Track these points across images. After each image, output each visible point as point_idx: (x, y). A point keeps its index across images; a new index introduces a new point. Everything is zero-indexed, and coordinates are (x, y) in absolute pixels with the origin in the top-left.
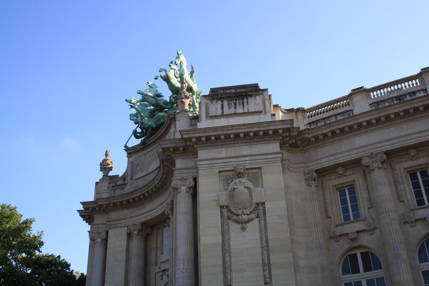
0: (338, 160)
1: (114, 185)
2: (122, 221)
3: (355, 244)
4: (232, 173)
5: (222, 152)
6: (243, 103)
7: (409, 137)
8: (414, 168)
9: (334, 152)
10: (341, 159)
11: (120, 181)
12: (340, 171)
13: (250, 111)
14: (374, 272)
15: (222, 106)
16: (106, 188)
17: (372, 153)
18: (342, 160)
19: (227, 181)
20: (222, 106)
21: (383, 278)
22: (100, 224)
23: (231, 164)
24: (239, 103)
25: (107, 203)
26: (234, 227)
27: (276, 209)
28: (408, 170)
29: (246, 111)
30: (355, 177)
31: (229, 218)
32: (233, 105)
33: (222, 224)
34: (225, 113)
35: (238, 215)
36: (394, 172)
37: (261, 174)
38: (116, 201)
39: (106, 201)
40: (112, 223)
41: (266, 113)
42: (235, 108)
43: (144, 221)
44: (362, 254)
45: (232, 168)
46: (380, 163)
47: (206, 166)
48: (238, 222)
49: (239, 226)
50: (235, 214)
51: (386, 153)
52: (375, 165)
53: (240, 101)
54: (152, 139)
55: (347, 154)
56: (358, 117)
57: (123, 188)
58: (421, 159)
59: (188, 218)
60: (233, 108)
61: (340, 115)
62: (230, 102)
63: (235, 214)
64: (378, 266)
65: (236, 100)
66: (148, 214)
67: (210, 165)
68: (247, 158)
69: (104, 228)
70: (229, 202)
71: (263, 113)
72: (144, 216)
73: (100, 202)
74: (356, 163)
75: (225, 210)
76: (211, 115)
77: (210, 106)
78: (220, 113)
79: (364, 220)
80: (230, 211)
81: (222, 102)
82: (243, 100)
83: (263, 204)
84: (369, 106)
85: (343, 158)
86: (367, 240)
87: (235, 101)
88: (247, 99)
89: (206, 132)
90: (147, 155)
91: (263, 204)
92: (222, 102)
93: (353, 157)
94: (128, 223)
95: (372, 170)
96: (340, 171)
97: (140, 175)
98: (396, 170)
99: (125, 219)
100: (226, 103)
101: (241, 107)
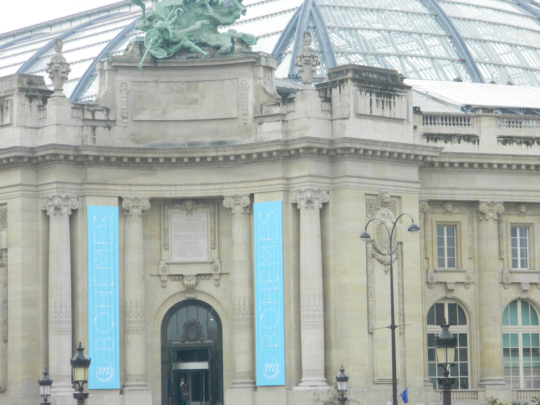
0: (452, 196)
1: (91, 118)
2: (110, 187)
3: (450, 295)
4: (374, 198)
6: (390, 102)
7: (528, 193)
8: (516, 225)
9: (452, 185)
10: (457, 196)
11: (100, 113)
12: (449, 207)
13: (396, 117)
14: (458, 326)
15: (371, 100)
16: (69, 117)
17: (493, 202)
18: (458, 198)
19: (371, 208)
20: (371, 100)
21: (466, 334)
22: (69, 183)
23: (376, 188)
24: (387, 101)
25: (96, 154)
28: (513, 225)
29: (393, 116)
31: (373, 257)
32: (381, 103)
33: (367, 260)
34: (373, 114)
35: (383, 254)
36: (501, 224)
37: (401, 205)
38: (111, 154)
39: (96, 151)
40: (93, 186)
41: (408, 122)
42: (383, 108)
43: (154, 196)
44: (449, 305)
45: (376, 193)
46: (496, 214)
47: (354, 184)
48: (382, 262)
49: (382, 267)
50: (379, 252)
51: (506, 204)
52: (491, 214)
53: (385, 99)
54: (176, 62)
55: (466, 192)
56: (493, 157)
57: (109, 128)
58: (527, 217)
60: (381, 108)
61: (464, 139)
62: (378, 99)
63: (379, 252)
64: (463, 322)
65: (384, 98)
66: (164, 188)
67: (357, 185)
68: (391, 183)
69: (73, 191)
70: (375, 237)
71: (405, 121)
72: (155, 188)
73: (86, 150)
75: (370, 246)
76: (360, 112)
77: (360, 98)
78: (368, 113)
79: (465, 272)
80: (374, 248)
81: (371, 95)
82: (390, 98)
83: (402, 243)
84: (496, 139)
86: (463, 295)
87: (382, 98)
88: (394, 99)
89: (367, 144)
90: (162, 86)
91: (402, 243)
92: (371, 95)
94: (121, 192)
95: (487, 220)
96: (449, 207)
97: (145, 116)
98: (502, 222)
99: (116, 184)
100: (374, 97)
101: (388, 108)
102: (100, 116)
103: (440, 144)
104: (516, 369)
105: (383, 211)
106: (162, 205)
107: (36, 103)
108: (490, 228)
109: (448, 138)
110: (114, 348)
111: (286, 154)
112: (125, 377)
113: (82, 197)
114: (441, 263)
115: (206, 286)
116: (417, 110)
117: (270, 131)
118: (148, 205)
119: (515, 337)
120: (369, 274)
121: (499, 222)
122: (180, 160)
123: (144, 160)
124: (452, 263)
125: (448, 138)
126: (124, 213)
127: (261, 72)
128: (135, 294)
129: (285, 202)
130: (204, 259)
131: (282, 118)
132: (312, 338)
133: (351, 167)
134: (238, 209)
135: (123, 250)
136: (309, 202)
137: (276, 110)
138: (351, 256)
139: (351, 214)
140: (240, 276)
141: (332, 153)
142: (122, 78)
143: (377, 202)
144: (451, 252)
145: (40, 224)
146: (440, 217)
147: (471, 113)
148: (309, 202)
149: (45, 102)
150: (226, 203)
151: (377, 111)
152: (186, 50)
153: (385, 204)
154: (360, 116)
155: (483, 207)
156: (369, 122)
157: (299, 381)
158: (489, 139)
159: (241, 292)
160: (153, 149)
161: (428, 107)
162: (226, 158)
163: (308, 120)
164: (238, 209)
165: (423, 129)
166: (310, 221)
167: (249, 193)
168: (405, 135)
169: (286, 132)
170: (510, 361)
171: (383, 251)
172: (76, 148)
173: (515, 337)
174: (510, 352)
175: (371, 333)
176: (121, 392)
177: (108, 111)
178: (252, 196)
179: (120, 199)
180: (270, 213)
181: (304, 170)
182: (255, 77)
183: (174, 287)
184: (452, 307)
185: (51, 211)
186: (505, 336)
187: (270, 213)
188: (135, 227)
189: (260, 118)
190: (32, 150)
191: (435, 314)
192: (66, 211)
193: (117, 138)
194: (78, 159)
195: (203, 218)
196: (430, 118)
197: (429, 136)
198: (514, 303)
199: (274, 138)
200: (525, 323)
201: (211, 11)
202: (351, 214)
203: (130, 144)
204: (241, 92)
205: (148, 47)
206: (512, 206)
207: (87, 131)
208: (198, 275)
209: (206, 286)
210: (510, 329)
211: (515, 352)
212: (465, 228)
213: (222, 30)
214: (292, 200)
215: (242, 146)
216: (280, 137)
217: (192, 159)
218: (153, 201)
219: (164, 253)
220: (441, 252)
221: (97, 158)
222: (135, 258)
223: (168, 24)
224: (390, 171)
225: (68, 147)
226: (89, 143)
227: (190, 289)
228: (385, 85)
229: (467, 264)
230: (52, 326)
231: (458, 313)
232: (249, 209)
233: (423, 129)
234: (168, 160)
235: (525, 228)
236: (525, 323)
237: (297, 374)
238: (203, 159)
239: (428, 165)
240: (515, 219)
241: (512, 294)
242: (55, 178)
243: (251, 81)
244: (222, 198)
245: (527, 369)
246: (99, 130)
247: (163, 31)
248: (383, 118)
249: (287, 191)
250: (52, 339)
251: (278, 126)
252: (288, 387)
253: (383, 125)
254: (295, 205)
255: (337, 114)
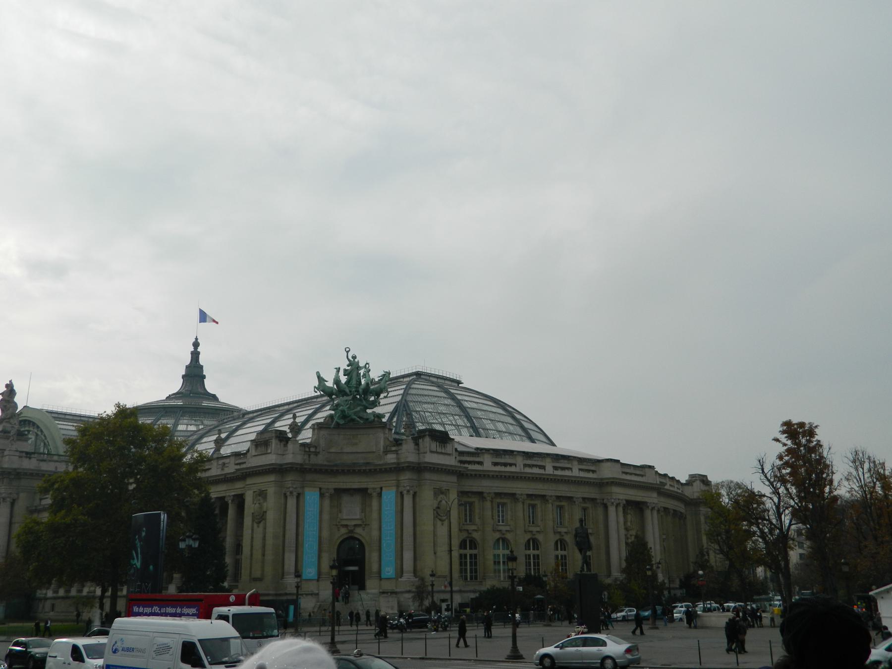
5: (435, 477)
26: (439, 523)
27: (454, 514)
30: (475, 499)
59: (411, 510)
64: (476, 548)
74: (480, 494)
85: (475, 489)
86: (475, 535)
93: (480, 490)
97: (333, 450)
102: (312, 450)
103: (466, 465)
104: (499, 571)
105: (441, 496)
106: (339, 492)
107: (282, 444)
108: (488, 504)
109: (469, 462)
110: (315, 559)
111: (398, 469)
112: (319, 573)
113: (303, 487)
114: (466, 521)
115: (359, 530)
116: (456, 450)
117: (391, 458)
118: (333, 491)
119: (499, 555)
120: (435, 526)
121: (492, 502)
122: (349, 471)
123: (332, 471)
124: (470, 521)
125: (469, 462)
126: (322, 495)
127: (387, 431)
128: (325, 534)
129: (397, 491)
130: (358, 517)
131: (396, 452)
132: (408, 556)
133: (427, 475)
134: (375, 494)
135: (321, 512)
136: (408, 491)
137: (394, 449)
138: (427, 517)
139: (427, 499)
140: (375, 525)
141: (419, 469)
142: (323, 432)
143: (438, 492)
144: (470, 515)
145: (283, 501)
146: (465, 499)
147: (480, 451)
148: (408, 491)
149: (287, 442)
150: (369, 491)
151: (439, 450)
152: (353, 420)
153: (442, 493)
154: (432, 452)
155: (485, 495)
156: (436, 455)
157: (401, 576)
158: (488, 464)
159: (375, 533)
160: (336, 465)
161: (460, 448)
162: (370, 470)
163: (408, 453)
164: (375, 494)
165: (458, 458)
166: (408, 500)
167: (379, 486)
168: (451, 461)
169: (398, 459)
170: (497, 567)
171: (440, 513)
172: (301, 465)
173: (499, 555)
174: (497, 563)
175: (435, 553)
176: (318, 580)
177: (316, 447)
178: (381, 488)
179: (320, 489)
180: (389, 497)
181: (406, 478)
182: (384, 433)
183: (343, 531)
184: (471, 542)
185: (288, 493)
186: (494, 555)
187: (389, 497)
188: (327, 502)
189: (386, 452)
190: (281, 465)
191: (463, 545)
192: (295, 494)
193: (320, 460)
194: (301, 470)
195: (358, 498)
196: (462, 453)
197: (461, 462)
198: (498, 540)
199: (393, 461)
200: (503, 549)
201: (364, 403)
202: (427, 499)
203: (325, 463)
204: (380, 439)
205: (336, 419)
206: (498, 495)
207: (306, 457)
208: (355, 526)
209: (359, 530)
210: (497, 552)
211: (499, 562)
212: (477, 505)
213: (369, 411)
214: (401, 489)
215: (379, 465)
216: (395, 461)
217: (354, 471)
218: (335, 489)
219: (340, 515)
220: (466, 515)
221: (310, 469)
222: (326, 517)
223: (345, 408)
224: (444, 478)
225: (297, 464)
226: (307, 462)
227: (351, 532)
228: (442, 438)
229: (477, 520)
230: (286, 549)
231: (473, 544)
232: (380, 495)
233: (458, 458)
234: (343, 471)
235: (503, 505)
236: (503, 549)
237: (400, 572)
238: (359, 470)
239: (462, 475)
240: (499, 500)
241: (497, 535)
242: (290, 480)
243: (382, 435)
244: (367, 489)
245: (504, 570)
246: (312, 456)
247: (343, 411)
248: (442, 453)
249: (398, 486)
250: (287, 555)
251: (394, 456)
252: (396, 579)
253: (441, 456)
254: (401, 493)
255: (422, 451)
